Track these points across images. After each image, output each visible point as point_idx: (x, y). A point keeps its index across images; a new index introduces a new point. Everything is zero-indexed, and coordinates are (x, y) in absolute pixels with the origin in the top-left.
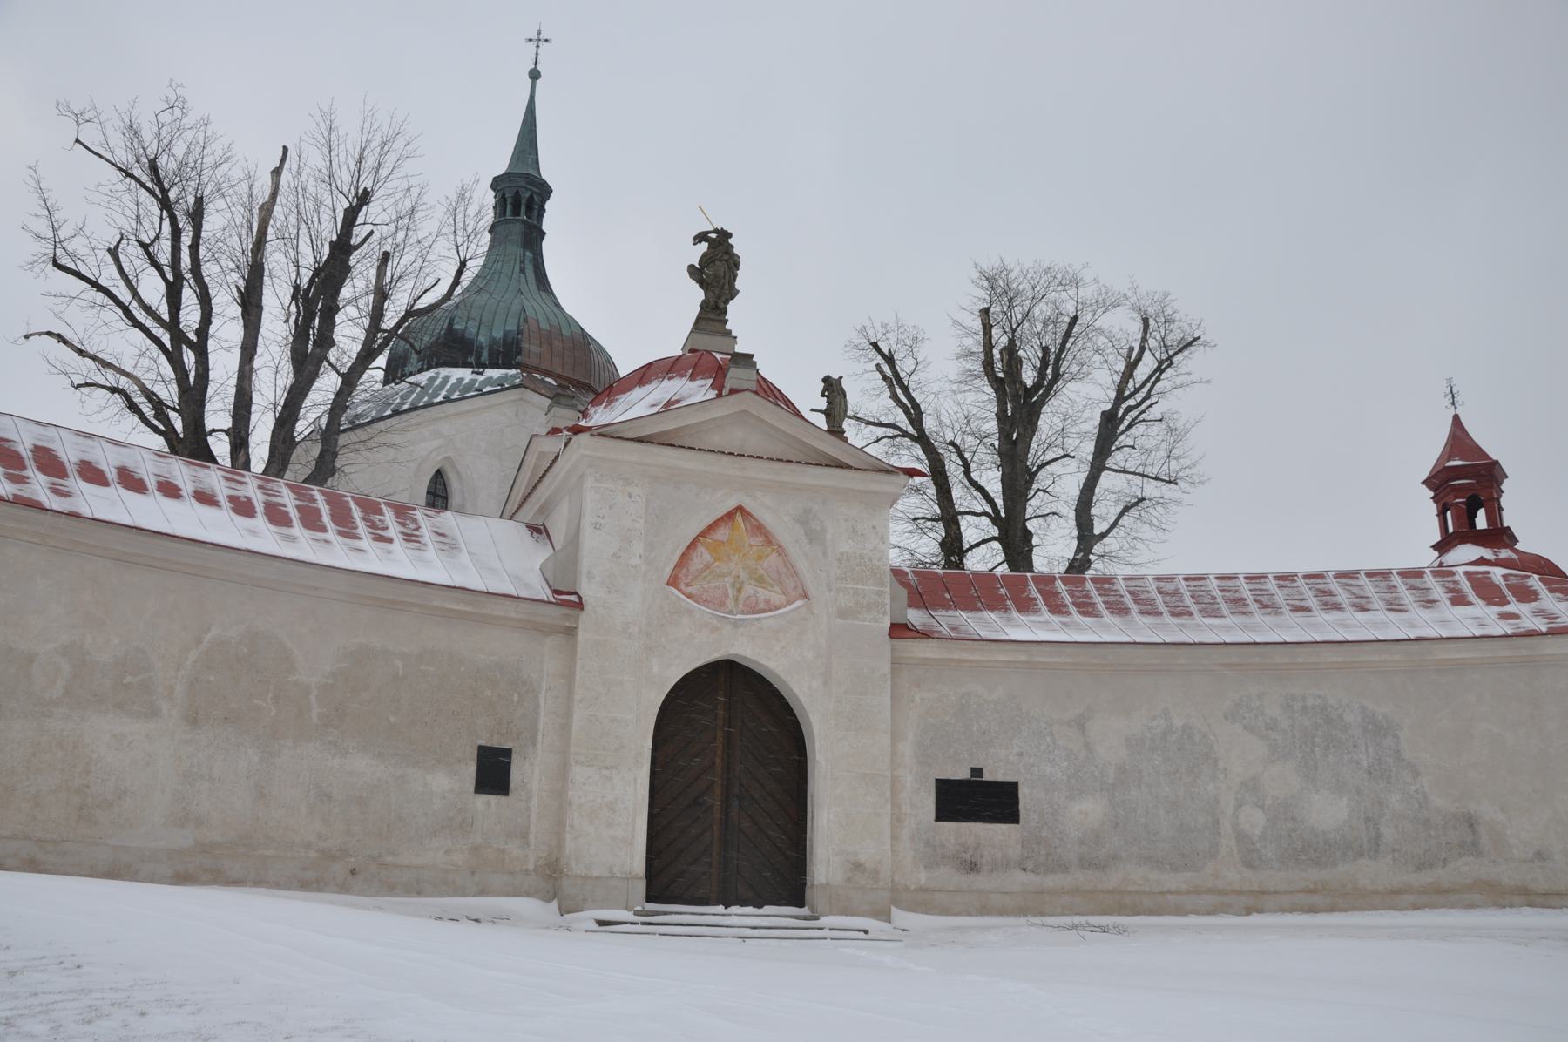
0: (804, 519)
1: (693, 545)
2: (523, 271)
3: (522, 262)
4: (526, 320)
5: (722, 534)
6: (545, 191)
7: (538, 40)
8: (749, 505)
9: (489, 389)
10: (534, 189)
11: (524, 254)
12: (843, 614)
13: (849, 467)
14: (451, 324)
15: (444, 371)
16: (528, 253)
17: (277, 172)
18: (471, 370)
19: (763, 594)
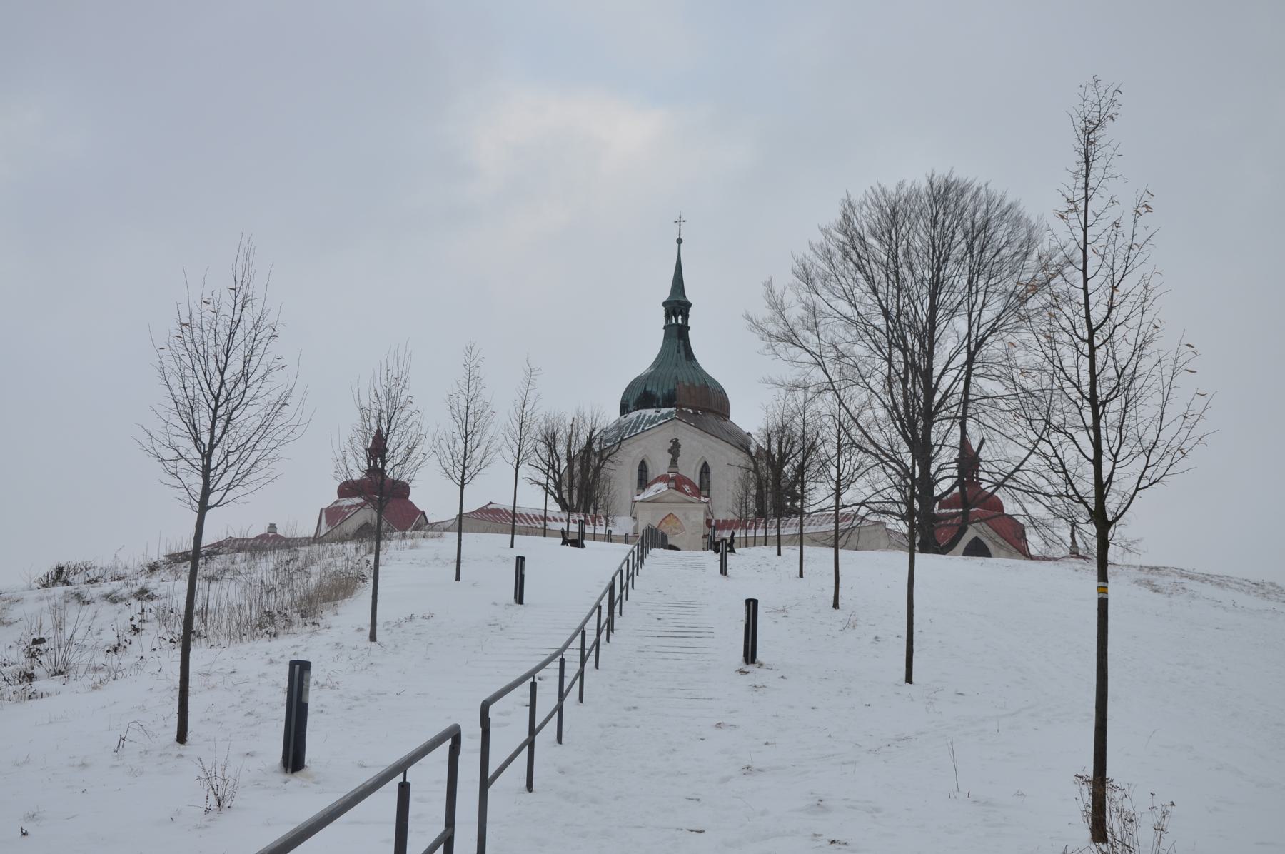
0: (685, 514)
1: (661, 522)
2: (679, 352)
3: (678, 346)
4: (678, 384)
5: (668, 519)
6: (690, 305)
7: (680, 221)
8: (673, 512)
9: (662, 421)
10: (683, 307)
11: (679, 343)
12: (693, 534)
13: (693, 503)
14: (645, 388)
15: (643, 412)
16: (681, 341)
17: (572, 425)
18: (654, 410)
19: (677, 531)
